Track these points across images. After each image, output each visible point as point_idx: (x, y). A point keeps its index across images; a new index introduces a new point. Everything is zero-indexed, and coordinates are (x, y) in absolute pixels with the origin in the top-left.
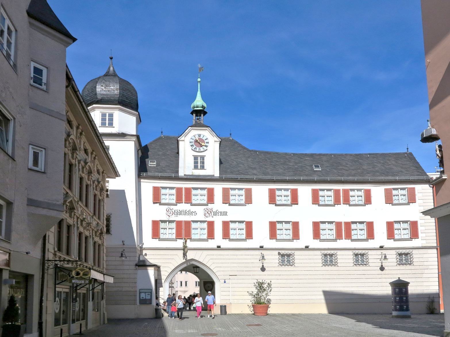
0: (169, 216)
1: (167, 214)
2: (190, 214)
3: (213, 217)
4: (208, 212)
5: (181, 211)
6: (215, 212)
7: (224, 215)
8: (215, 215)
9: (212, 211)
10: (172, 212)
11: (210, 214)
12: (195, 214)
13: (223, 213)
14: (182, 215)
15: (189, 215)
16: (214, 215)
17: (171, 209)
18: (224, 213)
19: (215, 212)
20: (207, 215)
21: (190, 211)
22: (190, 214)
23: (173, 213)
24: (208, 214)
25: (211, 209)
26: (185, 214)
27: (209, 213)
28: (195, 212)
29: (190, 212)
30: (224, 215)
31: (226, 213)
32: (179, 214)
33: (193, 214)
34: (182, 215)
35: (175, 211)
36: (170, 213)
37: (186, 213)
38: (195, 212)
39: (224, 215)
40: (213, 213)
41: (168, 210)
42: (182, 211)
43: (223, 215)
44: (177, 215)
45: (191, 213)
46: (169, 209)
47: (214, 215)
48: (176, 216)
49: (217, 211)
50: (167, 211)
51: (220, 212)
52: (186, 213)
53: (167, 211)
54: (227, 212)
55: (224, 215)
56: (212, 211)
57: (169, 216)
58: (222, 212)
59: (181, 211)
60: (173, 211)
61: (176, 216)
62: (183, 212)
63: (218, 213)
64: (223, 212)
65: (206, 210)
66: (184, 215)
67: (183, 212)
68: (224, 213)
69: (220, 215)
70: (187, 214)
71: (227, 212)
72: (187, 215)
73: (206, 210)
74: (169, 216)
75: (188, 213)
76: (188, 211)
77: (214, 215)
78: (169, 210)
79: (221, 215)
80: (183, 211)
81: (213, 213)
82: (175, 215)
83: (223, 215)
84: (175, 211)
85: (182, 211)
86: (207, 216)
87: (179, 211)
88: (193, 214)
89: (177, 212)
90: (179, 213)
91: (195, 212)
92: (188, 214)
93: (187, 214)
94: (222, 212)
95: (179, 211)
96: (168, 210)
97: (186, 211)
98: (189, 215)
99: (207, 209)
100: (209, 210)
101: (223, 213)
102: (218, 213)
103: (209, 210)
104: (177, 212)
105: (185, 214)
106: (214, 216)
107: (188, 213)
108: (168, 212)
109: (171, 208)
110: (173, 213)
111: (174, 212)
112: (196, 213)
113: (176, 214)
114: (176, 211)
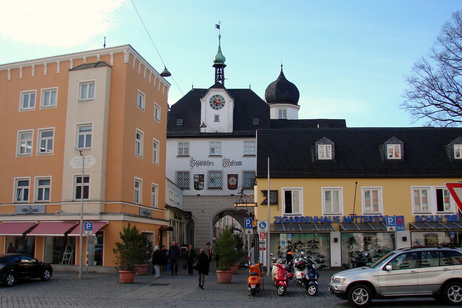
0: (192, 166)
3: (229, 167)
5: (201, 162)
7: (239, 165)
10: (194, 163)
11: (228, 164)
13: (238, 163)
14: (202, 165)
17: (194, 160)
19: (231, 162)
20: (225, 165)
23: (195, 164)
25: (228, 159)
29: (208, 163)
30: (239, 165)
31: (241, 163)
34: (202, 165)
35: (197, 162)
37: (205, 164)
40: (230, 162)
41: (191, 162)
42: (202, 162)
43: (238, 165)
44: (198, 166)
48: (197, 166)
50: (191, 162)
52: (205, 164)
53: (191, 162)
54: (241, 162)
55: (239, 165)
57: (192, 166)
58: (237, 162)
59: (201, 162)
61: (197, 166)
62: (203, 163)
63: (234, 163)
64: (239, 162)
66: (204, 165)
67: (203, 163)
69: (236, 165)
71: (241, 162)
74: (192, 167)
75: (207, 163)
77: (230, 165)
79: (237, 165)
82: (197, 165)
83: (238, 165)
84: (197, 162)
85: (202, 162)
89: (198, 163)
92: (207, 165)
94: (237, 162)
96: (191, 162)
97: (206, 162)
101: (238, 163)
102: (234, 163)
104: (198, 163)
107: (207, 163)
110: (195, 164)
111: (196, 163)
113: (197, 164)
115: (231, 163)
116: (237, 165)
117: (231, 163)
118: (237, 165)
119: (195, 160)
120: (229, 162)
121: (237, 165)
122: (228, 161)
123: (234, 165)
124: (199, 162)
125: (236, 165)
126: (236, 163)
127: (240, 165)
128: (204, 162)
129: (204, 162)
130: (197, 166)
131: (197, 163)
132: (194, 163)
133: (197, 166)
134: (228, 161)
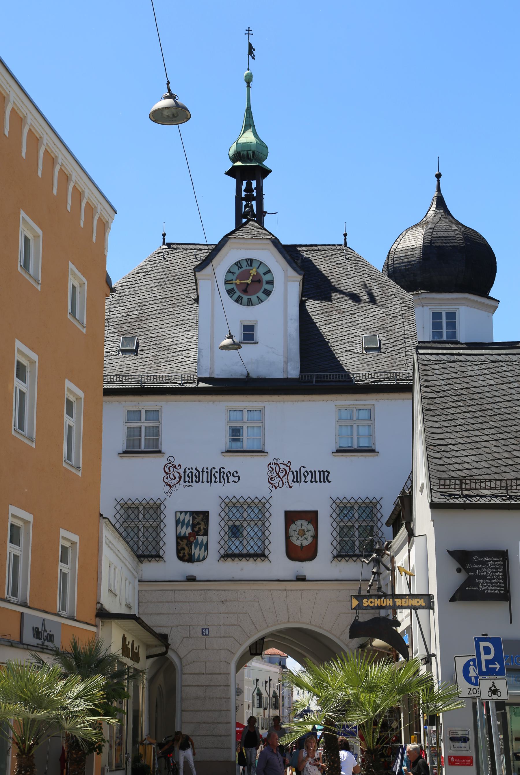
0: (169, 485)
1: (166, 480)
2: (222, 480)
3: (291, 487)
4: (278, 474)
5: (200, 471)
6: (296, 471)
7: (322, 480)
8: (298, 482)
9: (290, 469)
10: (177, 475)
12: (236, 479)
13: (318, 474)
14: (203, 482)
15: (220, 482)
16: (295, 480)
17: (175, 467)
18: (322, 473)
19: (296, 471)
21: (222, 470)
22: (222, 480)
23: (181, 478)
24: (279, 479)
25: (286, 463)
26: (209, 480)
27: (281, 475)
28: (237, 472)
29: (222, 474)
31: (326, 474)
32: (194, 478)
33: (231, 479)
34: (203, 482)
35: (185, 472)
36: (172, 477)
37: (213, 479)
38: (235, 474)
39: (320, 482)
40: (291, 474)
41: (167, 470)
42: (203, 471)
43: (318, 480)
44: (191, 484)
45: (225, 476)
46: (170, 465)
47: (295, 480)
49: (303, 470)
51: (311, 472)
53: (166, 473)
54: (329, 473)
55: (322, 480)
56: (290, 469)
57: (169, 485)
58: (315, 472)
59: (200, 471)
60: (181, 471)
61: (187, 484)
62: (205, 474)
63: (306, 474)
64: (319, 471)
65: (274, 466)
66: (208, 482)
67: (205, 474)
68: (322, 473)
69: (311, 482)
70: (216, 478)
71: (329, 473)
72: (215, 482)
73: (274, 466)
74: (171, 487)
75: (217, 475)
76: (218, 471)
77: (293, 481)
78: (171, 468)
79: (313, 480)
80: (205, 470)
81: (291, 475)
82: (185, 482)
83: (318, 480)
84: (185, 472)
85: (203, 471)
86: (277, 485)
87: (195, 472)
88: (231, 479)
90: (196, 477)
91: (235, 474)
92: (218, 480)
93: (216, 478)
94: (315, 472)
95: (195, 472)
96: (167, 470)
97: (214, 471)
98: (220, 482)
99: (275, 464)
100: (281, 466)
101: (318, 474)
102: (306, 474)
103: (281, 466)
104: (190, 475)
105: (209, 480)
106: (295, 485)
107: (217, 475)
108: (168, 475)
109: (175, 463)
110: (181, 478)
111: (183, 474)
112: (239, 477)
114: (188, 471)
115: (295, 473)
116: (316, 482)
117: (295, 473)
118: (313, 480)
119: (179, 465)
120: (288, 471)
121: (316, 482)
122: (287, 469)
123: (305, 482)
124: (192, 473)
125: (311, 482)
126: (310, 473)
127: (324, 482)
128: (207, 472)
129: (207, 472)
130: (185, 484)
131: (186, 474)
132: (177, 475)
133: (185, 484)
134: (287, 469)
